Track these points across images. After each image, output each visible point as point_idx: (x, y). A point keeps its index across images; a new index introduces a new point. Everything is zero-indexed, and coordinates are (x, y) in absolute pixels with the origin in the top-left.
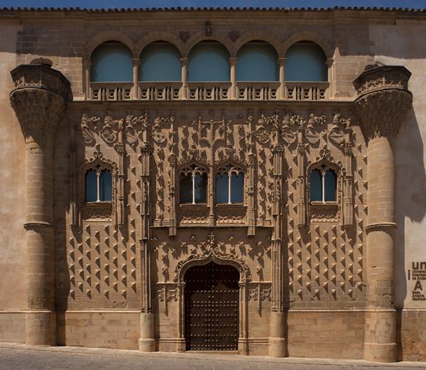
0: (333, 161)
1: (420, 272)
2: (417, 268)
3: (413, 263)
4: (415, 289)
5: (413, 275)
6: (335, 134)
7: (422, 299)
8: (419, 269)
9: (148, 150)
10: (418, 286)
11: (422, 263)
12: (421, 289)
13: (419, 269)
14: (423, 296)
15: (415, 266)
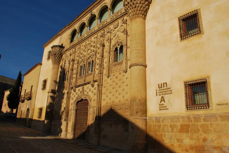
0: (120, 41)
1: (164, 89)
2: (161, 87)
3: (159, 85)
4: (161, 102)
5: (159, 92)
6: (122, 27)
7: (165, 109)
8: (163, 88)
9: (73, 60)
10: (163, 99)
11: (164, 84)
12: (165, 102)
13: (163, 88)
14: (166, 107)
15: (160, 86)
